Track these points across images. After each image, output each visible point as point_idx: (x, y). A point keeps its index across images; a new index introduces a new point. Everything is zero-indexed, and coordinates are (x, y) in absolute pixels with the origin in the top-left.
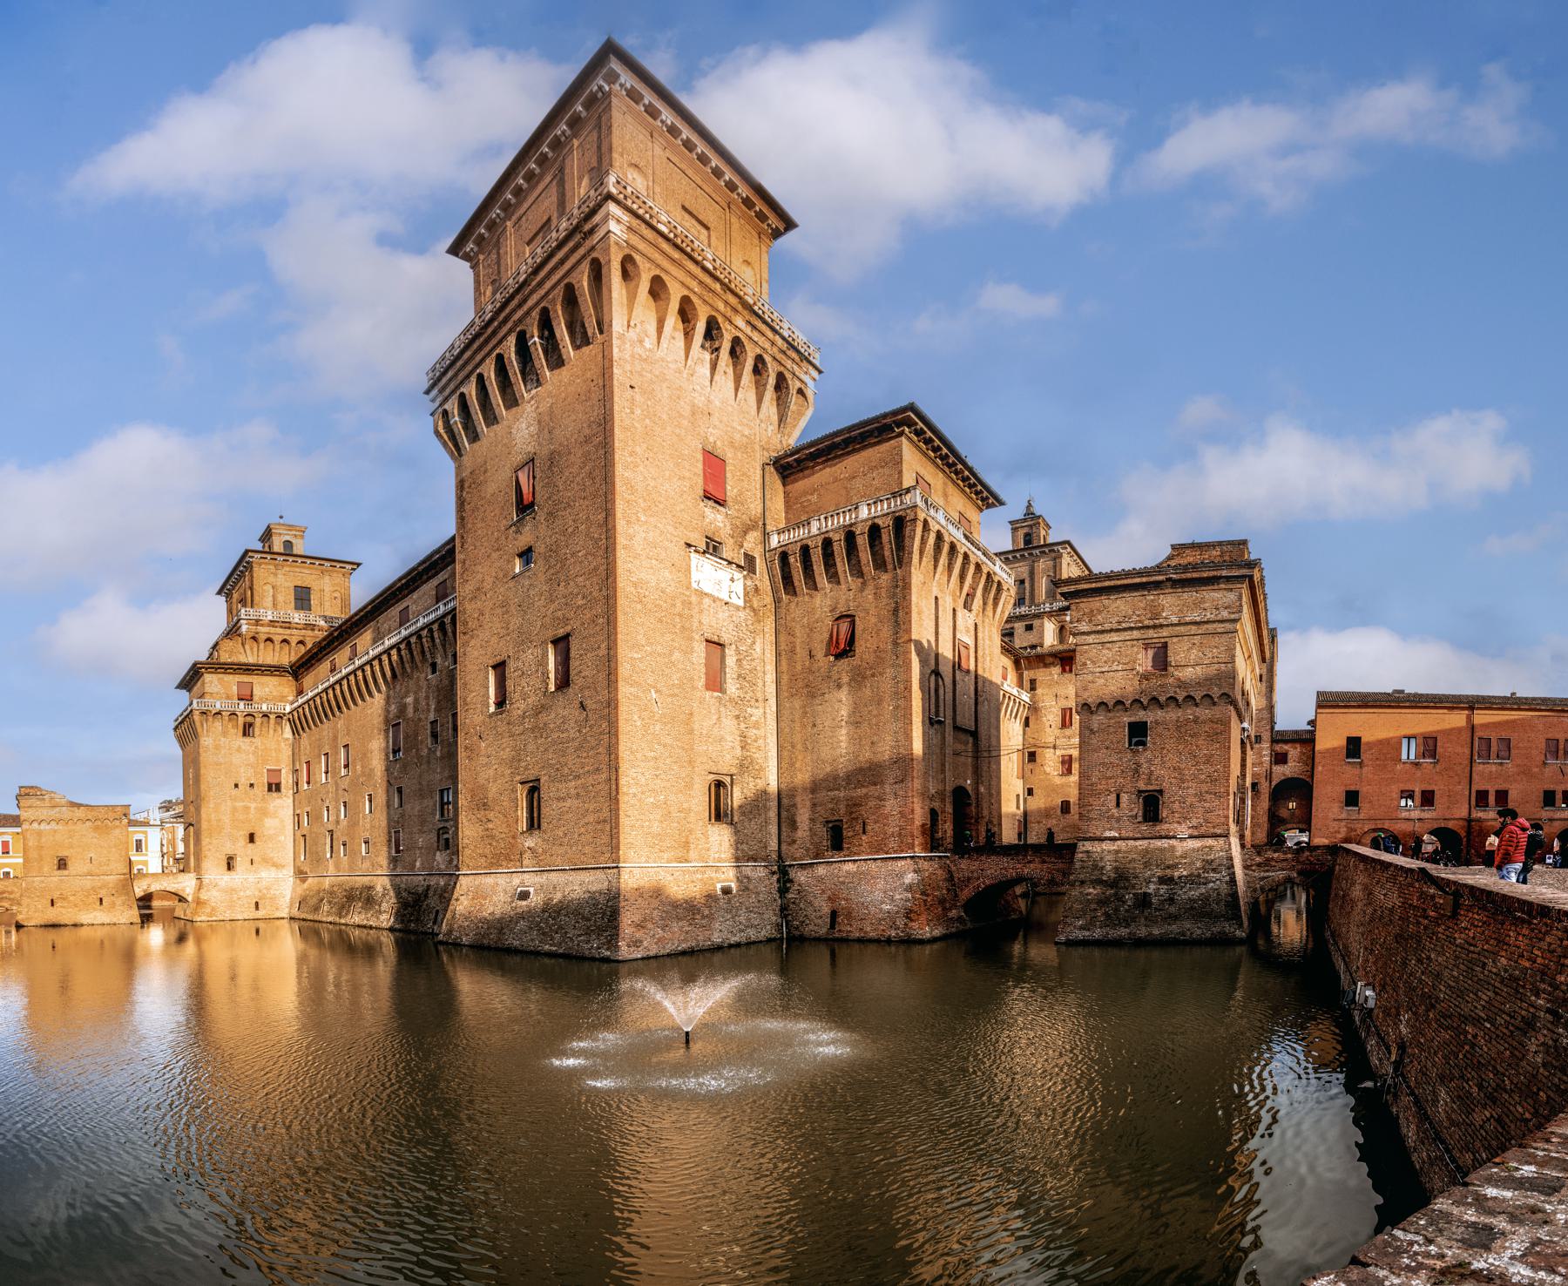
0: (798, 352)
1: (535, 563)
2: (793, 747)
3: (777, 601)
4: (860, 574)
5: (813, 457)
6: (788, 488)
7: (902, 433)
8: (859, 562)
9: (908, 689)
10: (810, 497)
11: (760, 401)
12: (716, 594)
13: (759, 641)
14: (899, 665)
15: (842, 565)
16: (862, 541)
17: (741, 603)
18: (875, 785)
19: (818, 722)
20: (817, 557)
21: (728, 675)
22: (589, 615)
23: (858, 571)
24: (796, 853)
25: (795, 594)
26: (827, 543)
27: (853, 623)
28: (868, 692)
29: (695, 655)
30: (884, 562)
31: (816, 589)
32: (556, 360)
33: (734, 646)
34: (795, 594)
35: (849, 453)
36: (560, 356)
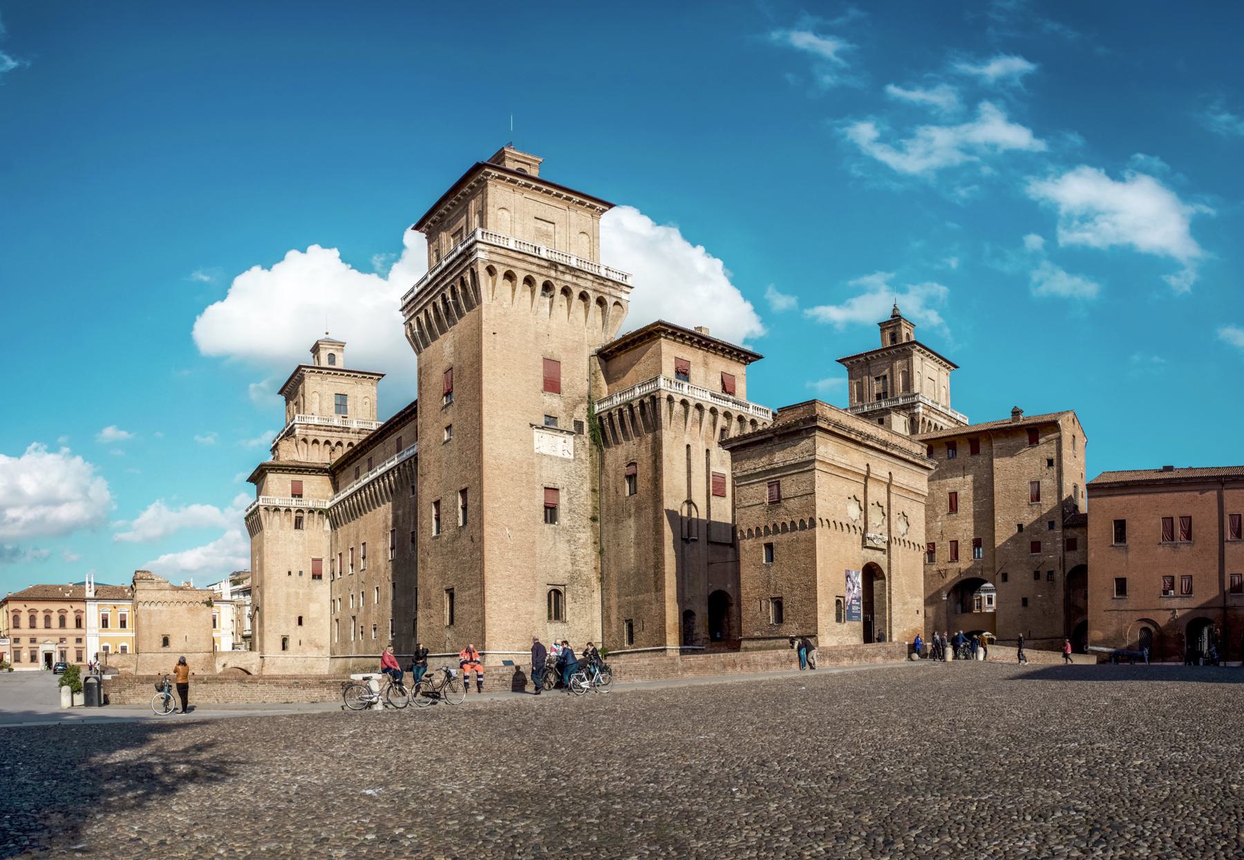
12: (553, 454)
17: (572, 457)
21: (561, 511)
29: (536, 500)
33: (566, 489)
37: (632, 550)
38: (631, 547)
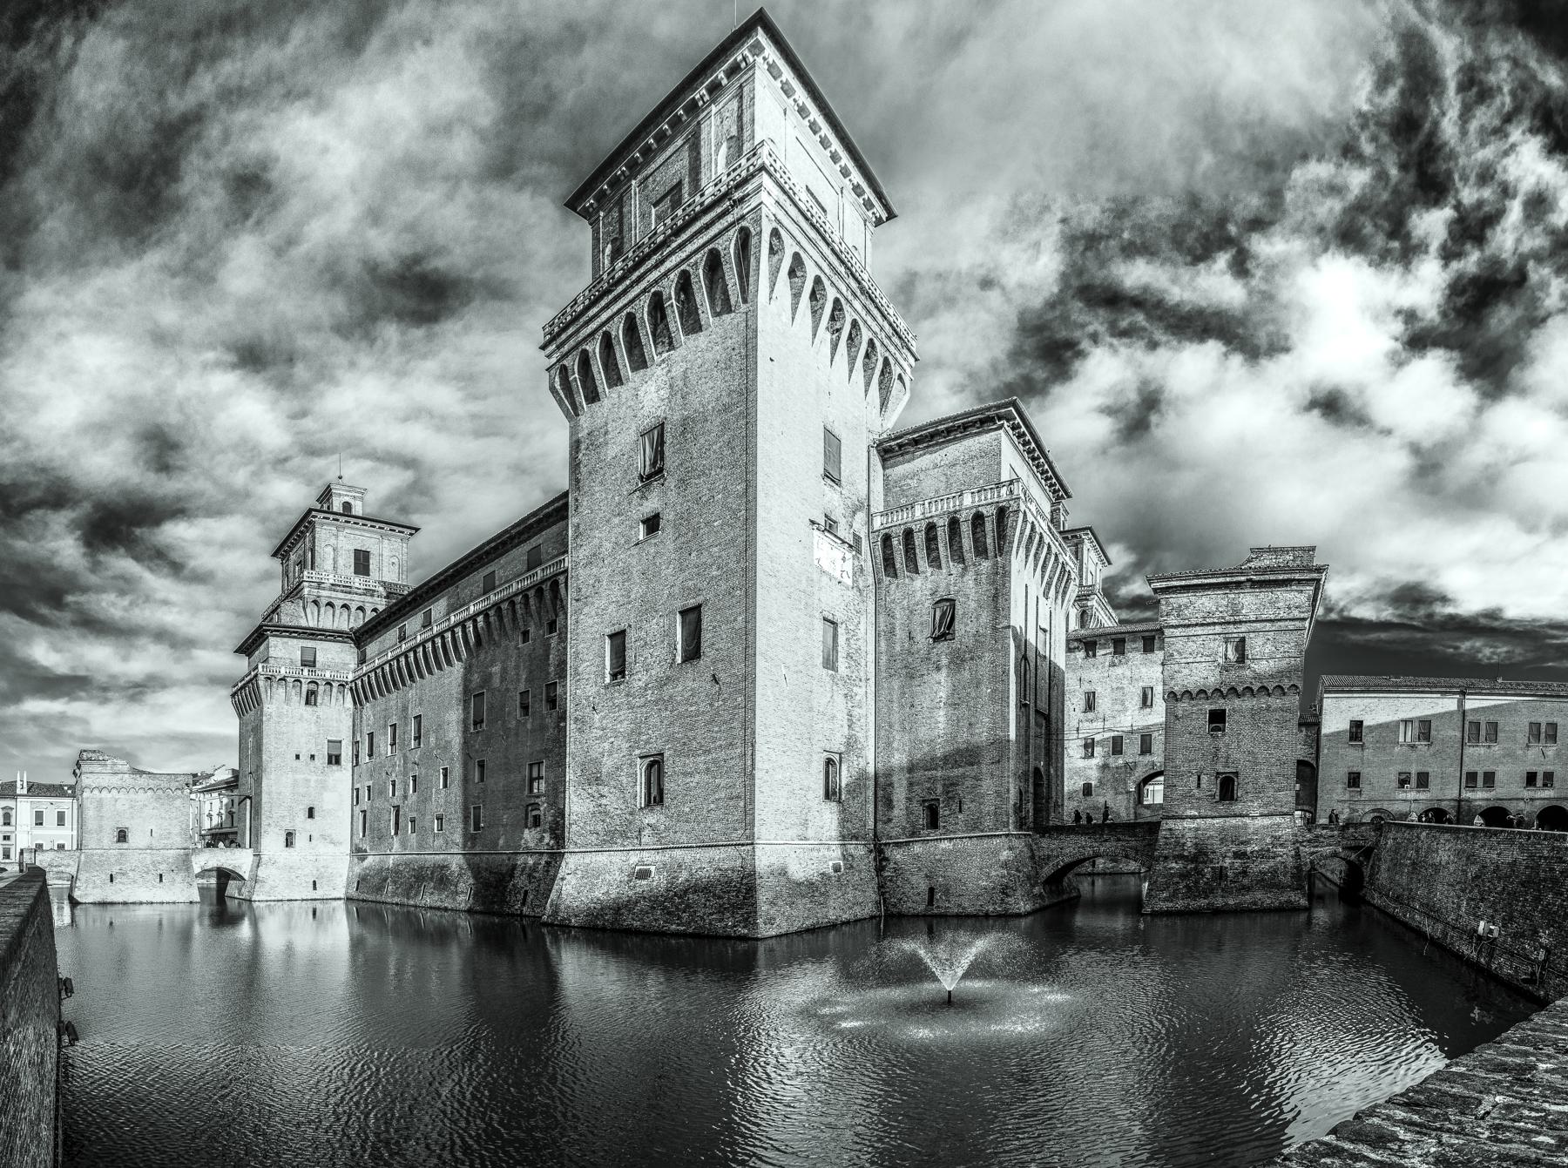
0: (900, 338)
1: (663, 530)
2: (890, 727)
3: (878, 582)
4: (962, 559)
5: (916, 442)
6: (888, 471)
7: (1001, 427)
8: (961, 547)
9: (1006, 673)
10: (909, 481)
11: (868, 384)
13: (863, 620)
14: (997, 650)
15: (943, 550)
16: (966, 529)
17: (849, 582)
18: (972, 764)
19: (916, 703)
20: (919, 540)
22: (724, 587)
23: (958, 556)
24: (894, 830)
25: (896, 576)
26: (931, 528)
27: (953, 607)
28: (966, 674)
30: (986, 550)
31: (917, 572)
32: (693, 325)
34: (896, 576)
35: (949, 441)
36: (698, 321)
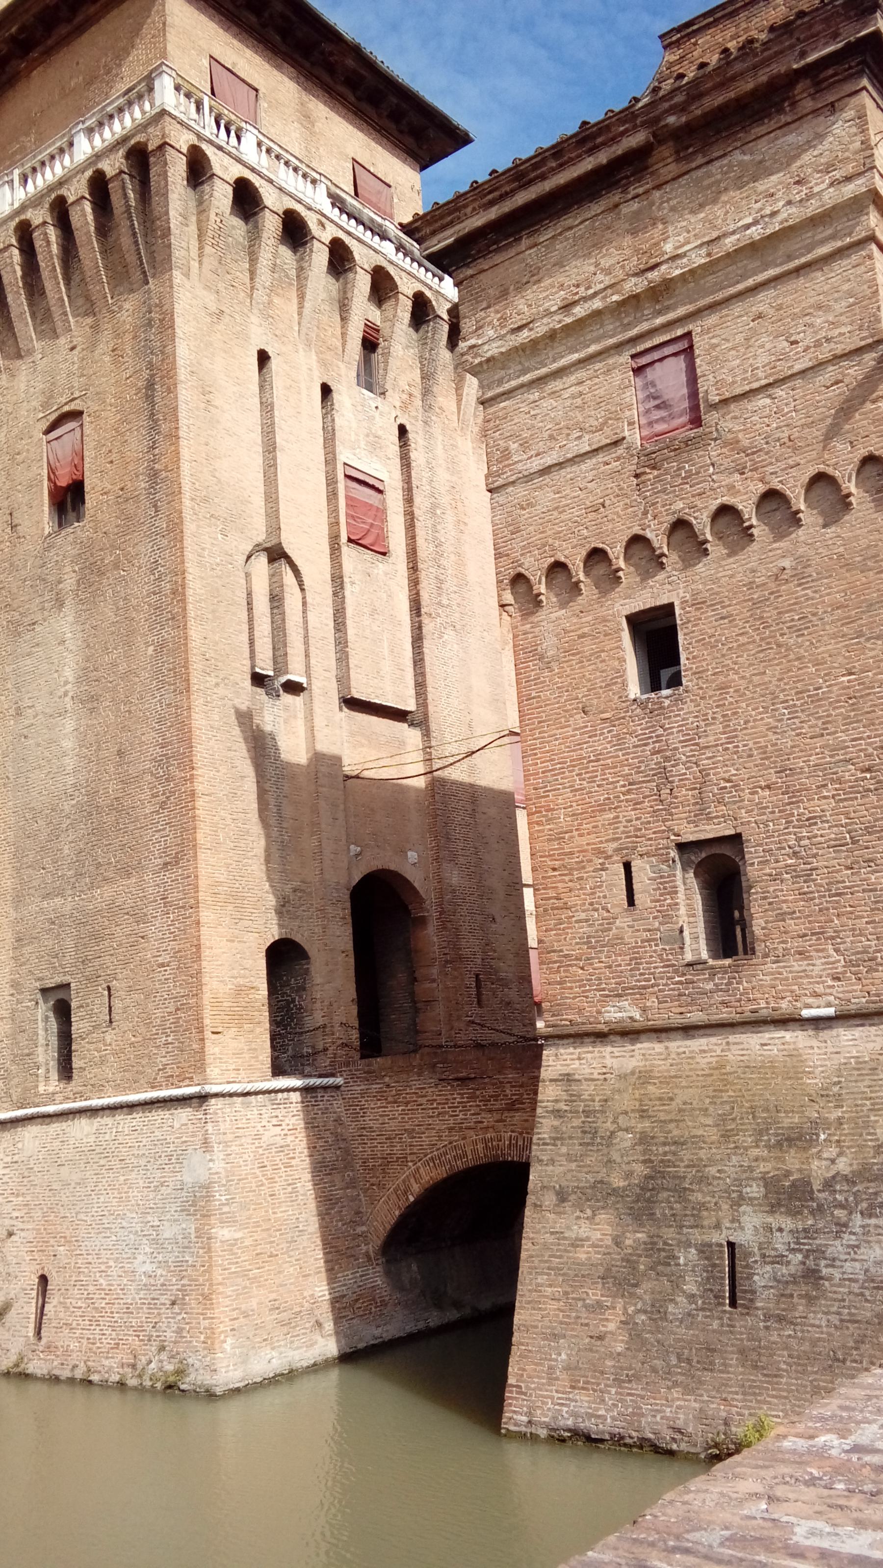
37: (69, 725)
38: (62, 714)
